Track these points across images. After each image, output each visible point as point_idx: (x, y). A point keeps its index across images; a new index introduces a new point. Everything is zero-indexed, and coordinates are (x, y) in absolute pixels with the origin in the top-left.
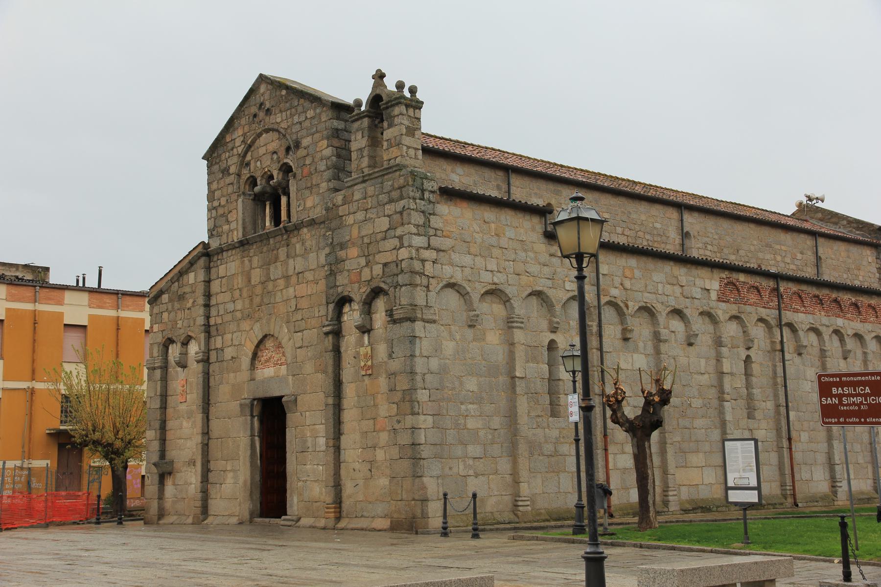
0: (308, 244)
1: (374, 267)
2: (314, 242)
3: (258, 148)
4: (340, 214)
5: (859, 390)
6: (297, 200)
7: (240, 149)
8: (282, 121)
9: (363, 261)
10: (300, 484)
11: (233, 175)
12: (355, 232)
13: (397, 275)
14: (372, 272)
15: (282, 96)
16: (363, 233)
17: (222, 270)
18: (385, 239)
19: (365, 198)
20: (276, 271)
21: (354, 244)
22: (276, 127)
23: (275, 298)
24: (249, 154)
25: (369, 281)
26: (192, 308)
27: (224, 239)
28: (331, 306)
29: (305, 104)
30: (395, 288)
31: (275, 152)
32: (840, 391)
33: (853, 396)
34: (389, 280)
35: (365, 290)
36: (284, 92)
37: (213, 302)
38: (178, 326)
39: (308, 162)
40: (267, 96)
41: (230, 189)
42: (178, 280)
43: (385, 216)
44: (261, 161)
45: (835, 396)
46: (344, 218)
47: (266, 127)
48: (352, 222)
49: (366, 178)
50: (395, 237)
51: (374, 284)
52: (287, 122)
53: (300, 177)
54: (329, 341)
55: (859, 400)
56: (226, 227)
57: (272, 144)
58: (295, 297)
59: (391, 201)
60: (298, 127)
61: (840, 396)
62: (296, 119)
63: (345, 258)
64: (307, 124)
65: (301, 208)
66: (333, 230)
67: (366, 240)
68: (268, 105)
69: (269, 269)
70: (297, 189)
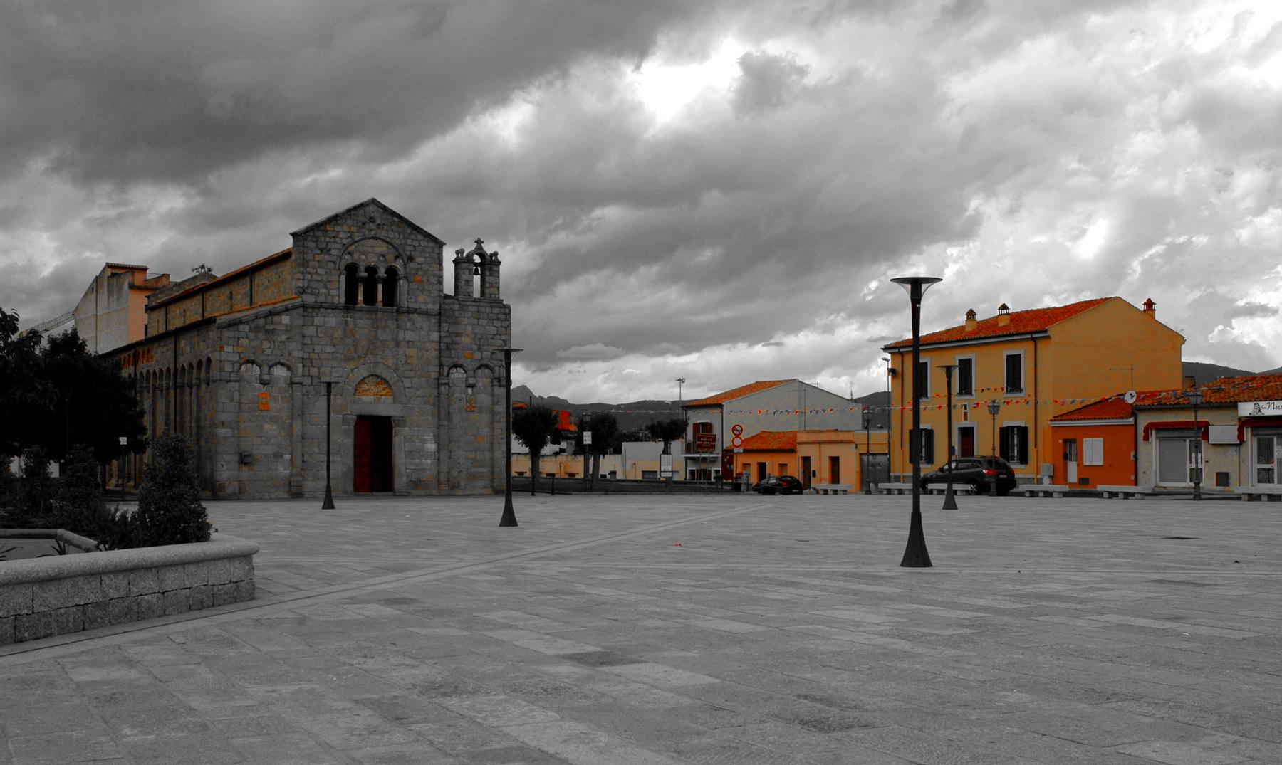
0: (419, 325)
2: (425, 325)
3: (363, 245)
6: (408, 294)
7: (345, 241)
8: (395, 238)
9: (476, 348)
10: (408, 471)
15: (394, 221)
16: (476, 331)
17: (317, 321)
18: (492, 339)
20: (383, 335)
21: (467, 335)
22: (388, 240)
24: (353, 246)
25: (479, 360)
27: (321, 299)
28: (446, 369)
31: (383, 256)
35: (477, 364)
36: (396, 219)
38: (266, 353)
39: (420, 273)
41: (331, 265)
42: (266, 317)
43: (493, 326)
46: (460, 319)
47: (378, 236)
51: (485, 362)
54: (445, 388)
56: (324, 291)
59: (498, 319)
60: (413, 249)
62: (409, 242)
65: (412, 300)
66: (450, 324)
68: (378, 221)
69: (376, 332)
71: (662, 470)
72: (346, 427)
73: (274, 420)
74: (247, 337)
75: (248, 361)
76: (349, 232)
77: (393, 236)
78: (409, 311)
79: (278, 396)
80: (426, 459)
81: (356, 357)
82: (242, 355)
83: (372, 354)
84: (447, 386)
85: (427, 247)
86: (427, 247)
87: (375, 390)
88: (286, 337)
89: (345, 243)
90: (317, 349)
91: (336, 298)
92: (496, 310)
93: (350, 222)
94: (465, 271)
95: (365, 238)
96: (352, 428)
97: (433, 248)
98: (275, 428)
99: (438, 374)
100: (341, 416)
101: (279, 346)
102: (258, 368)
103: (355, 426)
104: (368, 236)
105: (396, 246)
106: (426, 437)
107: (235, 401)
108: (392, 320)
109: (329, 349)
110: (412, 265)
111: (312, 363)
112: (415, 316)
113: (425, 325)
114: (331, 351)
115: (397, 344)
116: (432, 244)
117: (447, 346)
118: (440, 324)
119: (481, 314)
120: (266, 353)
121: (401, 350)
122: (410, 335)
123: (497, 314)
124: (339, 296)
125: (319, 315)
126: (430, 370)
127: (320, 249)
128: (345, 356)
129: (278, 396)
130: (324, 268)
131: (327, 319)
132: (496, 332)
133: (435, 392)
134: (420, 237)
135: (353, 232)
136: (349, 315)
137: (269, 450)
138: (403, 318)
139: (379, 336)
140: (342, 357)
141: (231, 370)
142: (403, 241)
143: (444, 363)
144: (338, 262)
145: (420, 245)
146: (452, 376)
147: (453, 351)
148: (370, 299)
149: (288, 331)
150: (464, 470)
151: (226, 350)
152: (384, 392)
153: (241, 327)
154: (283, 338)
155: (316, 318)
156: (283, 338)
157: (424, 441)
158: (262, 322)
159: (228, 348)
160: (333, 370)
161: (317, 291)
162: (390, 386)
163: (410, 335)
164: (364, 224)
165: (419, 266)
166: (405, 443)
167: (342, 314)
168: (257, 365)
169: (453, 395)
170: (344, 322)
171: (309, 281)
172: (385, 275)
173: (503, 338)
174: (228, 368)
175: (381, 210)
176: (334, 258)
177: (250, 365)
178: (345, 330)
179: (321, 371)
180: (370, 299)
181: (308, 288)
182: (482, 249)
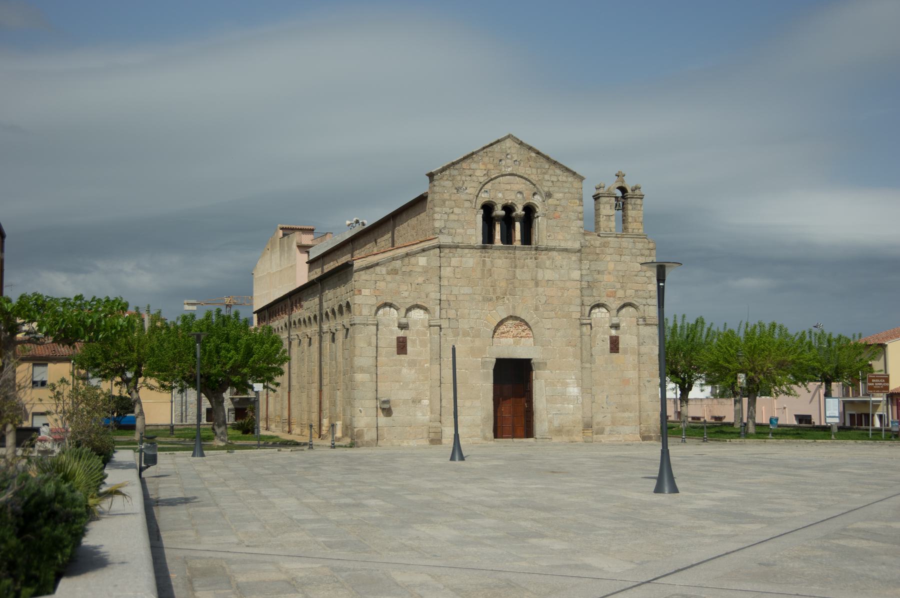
1: (627, 291)
2: (564, 263)
4: (597, 252)
5: (881, 381)
7: (482, 179)
9: (618, 285)
11: (471, 195)
12: (611, 266)
13: (646, 299)
14: (625, 293)
15: (531, 157)
17: (455, 261)
18: (636, 276)
19: (620, 248)
23: (523, 292)
26: (423, 285)
27: (458, 240)
28: (588, 309)
29: (556, 171)
30: (644, 305)
31: (520, 193)
32: (875, 381)
33: (878, 382)
34: (640, 300)
35: (620, 303)
36: (533, 155)
37: (445, 282)
39: (559, 209)
40: (513, 151)
41: (467, 204)
43: (637, 263)
44: (503, 194)
45: (873, 382)
47: (515, 173)
48: (609, 260)
49: (618, 236)
50: (645, 276)
52: (538, 177)
53: (551, 218)
54: (587, 329)
55: (880, 384)
57: (518, 186)
58: (545, 295)
59: (642, 255)
60: (550, 184)
61: (875, 383)
62: (547, 177)
63: (602, 280)
64: (559, 184)
65: (550, 238)
66: (591, 261)
67: (621, 273)
69: (515, 271)
70: (547, 224)
71: (827, 415)
72: (485, 370)
73: (412, 364)
74: (384, 280)
75: (386, 305)
76: (485, 170)
77: (529, 172)
78: (548, 249)
79: (416, 339)
80: (568, 404)
81: (494, 298)
82: (379, 298)
83: (510, 294)
84: (589, 327)
85: (566, 182)
86: (566, 182)
87: (515, 332)
88: (423, 279)
89: (482, 181)
90: (455, 291)
91: (474, 238)
92: (639, 246)
93: (486, 159)
94: (607, 205)
95: (502, 176)
96: (492, 372)
97: (571, 183)
98: (413, 371)
99: (579, 314)
100: (480, 359)
101: (416, 289)
102: (395, 311)
103: (494, 370)
104: (505, 173)
105: (534, 182)
106: (568, 381)
107: (373, 345)
108: (531, 258)
109: (466, 290)
110: (550, 201)
111: (449, 305)
112: (554, 253)
113: (564, 263)
114: (468, 293)
115: (537, 284)
116: (571, 179)
117: (589, 285)
118: (581, 260)
119: (624, 250)
120: (403, 295)
121: (540, 290)
122: (549, 274)
123: (641, 250)
124: (476, 235)
125: (456, 255)
126: (570, 310)
127: (456, 189)
128: (483, 297)
129: (416, 339)
130: (460, 208)
131: (464, 259)
132: (640, 269)
133: (578, 333)
134: (558, 171)
135: (489, 170)
136: (487, 254)
137: (406, 395)
138: (543, 256)
139: (517, 275)
140: (481, 298)
141: (369, 314)
142: (541, 177)
143: (585, 303)
144: (475, 200)
145: (558, 180)
146: (594, 316)
147: (594, 290)
148: (508, 239)
149: (425, 272)
150: (609, 415)
151: (363, 294)
152: (524, 334)
153: (378, 269)
154: (420, 280)
155: (452, 259)
156: (420, 280)
157: (566, 385)
158: (398, 263)
159: (366, 292)
160: (471, 311)
161: (454, 231)
162: (529, 327)
163: (549, 274)
164: (500, 160)
165: (558, 202)
166: (546, 387)
167: (479, 254)
168: (394, 309)
169: (595, 336)
170: (481, 262)
171: (446, 221)
172: (524, 213)
173: (647, 275)
174: (365, 312)
175: (517, 145)
176: (471, 197)
177: (387, 309)
178: (483, 271)
179: (458, 313)
180: (508, 239)
181: (445, 228)
182: (623, 181)
